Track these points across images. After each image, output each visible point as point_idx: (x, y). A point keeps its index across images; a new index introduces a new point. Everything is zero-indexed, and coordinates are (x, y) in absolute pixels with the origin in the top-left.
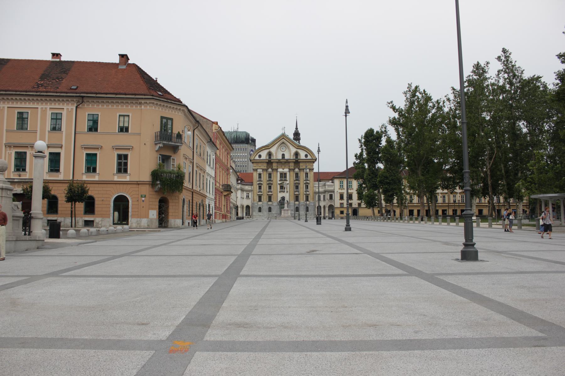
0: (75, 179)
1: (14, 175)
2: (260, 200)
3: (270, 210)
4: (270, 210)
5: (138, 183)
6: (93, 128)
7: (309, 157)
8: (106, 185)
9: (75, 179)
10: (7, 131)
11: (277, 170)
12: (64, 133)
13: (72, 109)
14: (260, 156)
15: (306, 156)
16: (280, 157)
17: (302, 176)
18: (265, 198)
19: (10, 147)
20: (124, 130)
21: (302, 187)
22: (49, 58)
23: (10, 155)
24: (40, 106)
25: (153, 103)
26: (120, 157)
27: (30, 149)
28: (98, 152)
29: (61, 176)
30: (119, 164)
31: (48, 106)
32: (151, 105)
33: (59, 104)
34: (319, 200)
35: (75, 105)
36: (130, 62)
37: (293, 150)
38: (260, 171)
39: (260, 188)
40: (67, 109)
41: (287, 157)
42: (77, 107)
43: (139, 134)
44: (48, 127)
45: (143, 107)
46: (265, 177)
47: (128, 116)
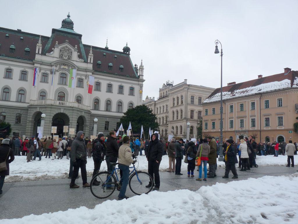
0: (261, 129)
1: (240, 129)
5: (287, 130)
6: (267, 106)
8: (273, 132)
9: (261, 129)
10: (237, 112)
12: (256, 111)
13: (258, 100)
19: (238, 118)
22: (257, 78)
23: (238, 121)
24: (247, 101)
25: (292, 91)
26: (279, 118)
27: (244, 118)
28: (270, 117)
29: (256, 128)
30: (280, 121)
31: (250, 100)
32: (292, 91)
33: (241, 101)
35: (259, 98)
36: (292, 70)
42: (260, 98)
43: (287, 107)
44: (250, 108)
45: (288, 93)
47: (282, 98)
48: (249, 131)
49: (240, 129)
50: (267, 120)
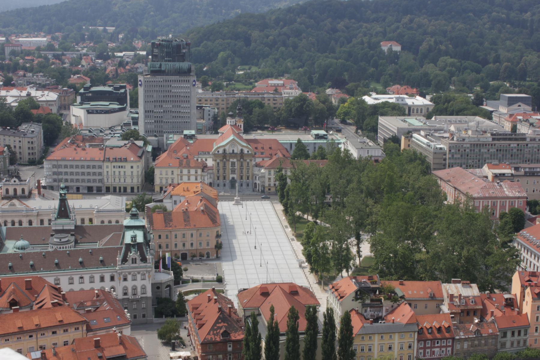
2: (218, 179)
3: (224, 185)
4: (224, 185)
5: (212, 249)
7: (250, 152)
11: (229, 161)
14: (218, 152)
15: (248, 152)
16: (231, 152)
17: (245, 164)
18: (221, 178)
20: (208, 236)
21: (244, 171)
29: (194, 248)
34: (255, 179)
37: (240, 148)
38: (218, 161)
39: (218, 171)
40: (194, 232)
41: (235, 152)
46: (221, 165)
48: (189, 250)
49: (182, 249)
50: (200, 243)
